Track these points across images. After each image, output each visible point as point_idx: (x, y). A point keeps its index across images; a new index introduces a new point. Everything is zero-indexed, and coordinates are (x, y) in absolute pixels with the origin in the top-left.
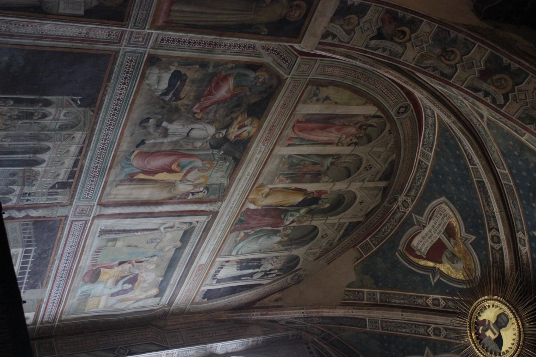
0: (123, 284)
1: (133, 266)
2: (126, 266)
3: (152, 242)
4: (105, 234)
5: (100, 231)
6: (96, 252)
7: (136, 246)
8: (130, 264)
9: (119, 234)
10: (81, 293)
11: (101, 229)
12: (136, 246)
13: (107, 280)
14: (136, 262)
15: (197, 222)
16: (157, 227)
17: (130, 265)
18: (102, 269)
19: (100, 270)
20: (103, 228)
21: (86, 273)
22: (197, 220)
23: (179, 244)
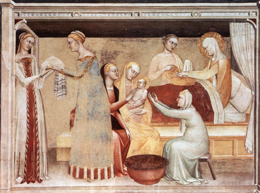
0: (178, 108)
1: (126, 102)
3: (64, 87)
4: (37, 172)
5: (28, 183)
6: (81, 177)
7: (73, 112)
8: (120, 110)
9: (37, 149)
10: (193, 176)
11: (22, 182)
12: (73, 112)
13: (162, 139)
14: (117, 99)
15: (16, 21)
16: (25, 89)
17: (123, 110)
18: (130, 154)
19: (131, 158)
20: (20, 179)
21: (137, 180)
22: (11, 21)
23: (75, 35)
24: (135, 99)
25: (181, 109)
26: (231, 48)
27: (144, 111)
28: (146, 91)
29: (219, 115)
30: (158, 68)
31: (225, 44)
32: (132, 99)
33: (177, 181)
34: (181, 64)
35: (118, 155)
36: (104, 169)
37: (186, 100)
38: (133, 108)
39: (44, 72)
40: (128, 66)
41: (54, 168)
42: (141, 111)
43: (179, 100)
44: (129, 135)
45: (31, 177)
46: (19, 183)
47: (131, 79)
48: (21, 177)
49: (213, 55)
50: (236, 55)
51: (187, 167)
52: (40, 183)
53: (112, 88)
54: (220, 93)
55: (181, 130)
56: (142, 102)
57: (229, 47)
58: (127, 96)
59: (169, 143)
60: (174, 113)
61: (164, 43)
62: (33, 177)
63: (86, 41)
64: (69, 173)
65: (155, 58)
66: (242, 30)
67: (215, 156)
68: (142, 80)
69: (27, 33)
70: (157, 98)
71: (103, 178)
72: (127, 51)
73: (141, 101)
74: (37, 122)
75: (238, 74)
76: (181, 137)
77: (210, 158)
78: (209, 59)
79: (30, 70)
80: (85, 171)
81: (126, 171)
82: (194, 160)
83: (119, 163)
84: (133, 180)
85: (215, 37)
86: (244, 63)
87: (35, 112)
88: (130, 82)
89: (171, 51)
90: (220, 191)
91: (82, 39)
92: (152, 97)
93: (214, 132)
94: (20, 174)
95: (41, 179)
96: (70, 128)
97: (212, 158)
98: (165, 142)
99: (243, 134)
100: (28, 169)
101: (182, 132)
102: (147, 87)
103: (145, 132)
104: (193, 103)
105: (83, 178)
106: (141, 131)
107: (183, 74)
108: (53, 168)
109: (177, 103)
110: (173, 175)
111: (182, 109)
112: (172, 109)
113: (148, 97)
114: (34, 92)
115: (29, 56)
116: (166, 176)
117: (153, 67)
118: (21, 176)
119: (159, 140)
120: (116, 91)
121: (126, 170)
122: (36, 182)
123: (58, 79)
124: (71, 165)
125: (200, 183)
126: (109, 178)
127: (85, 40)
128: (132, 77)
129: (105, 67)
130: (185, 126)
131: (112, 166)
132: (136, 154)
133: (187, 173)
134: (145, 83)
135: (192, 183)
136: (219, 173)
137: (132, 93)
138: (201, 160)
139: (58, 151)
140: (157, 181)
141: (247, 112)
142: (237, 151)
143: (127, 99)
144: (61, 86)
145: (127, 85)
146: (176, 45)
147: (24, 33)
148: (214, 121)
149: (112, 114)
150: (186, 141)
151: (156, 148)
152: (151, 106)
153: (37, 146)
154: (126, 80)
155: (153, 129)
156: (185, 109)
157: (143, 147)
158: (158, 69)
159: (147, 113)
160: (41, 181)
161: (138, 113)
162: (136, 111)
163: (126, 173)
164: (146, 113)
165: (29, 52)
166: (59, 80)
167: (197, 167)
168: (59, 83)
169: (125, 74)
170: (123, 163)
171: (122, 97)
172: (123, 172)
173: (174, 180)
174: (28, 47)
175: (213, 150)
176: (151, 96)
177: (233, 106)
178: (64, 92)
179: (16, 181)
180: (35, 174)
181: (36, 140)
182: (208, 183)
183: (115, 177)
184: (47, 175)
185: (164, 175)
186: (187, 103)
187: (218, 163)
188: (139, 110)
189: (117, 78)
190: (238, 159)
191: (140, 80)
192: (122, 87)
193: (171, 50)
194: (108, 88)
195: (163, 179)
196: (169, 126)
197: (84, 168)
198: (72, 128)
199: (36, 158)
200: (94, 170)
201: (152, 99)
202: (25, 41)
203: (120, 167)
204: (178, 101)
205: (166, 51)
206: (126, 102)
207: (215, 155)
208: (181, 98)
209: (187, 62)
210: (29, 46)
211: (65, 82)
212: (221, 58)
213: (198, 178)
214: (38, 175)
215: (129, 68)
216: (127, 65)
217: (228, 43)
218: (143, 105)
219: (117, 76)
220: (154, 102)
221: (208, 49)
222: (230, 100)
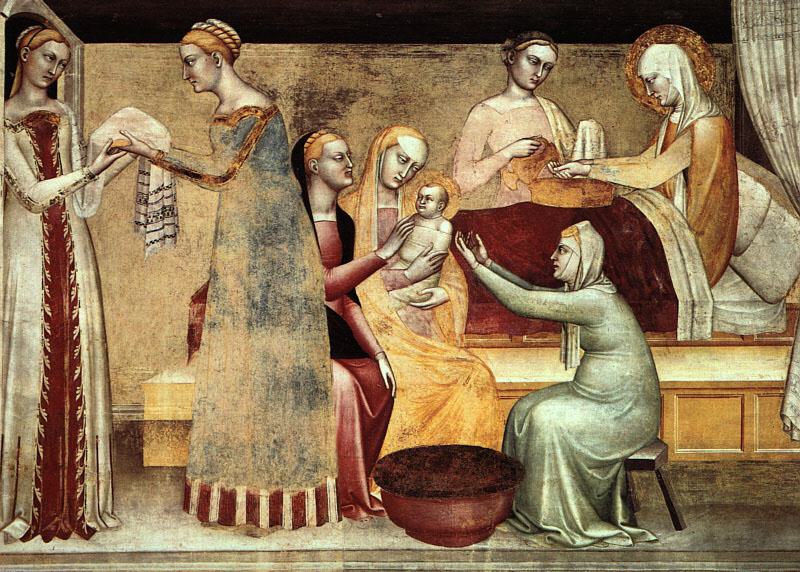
0: (557, 285)
1: (379, 264)
2: (376, 305)
3: (169, 211)
6: (227, 519)
7: (200, 297)
8: (359, 290)
9: (77, 425)
10: (608, 518)
11: (26, 538)
14: (346, 254)
16: (36, 219)
17: (370, 290)
18: (391, 445)
19: (396, 456)
20: (19, 527)
21: (415, 532)
24: (409, 253)
25: (566, 287)
26: (737, 81)
27: (440, 294)
28: (447, 227)
29: (696, 309)
30: (487, 147)
31: (717, 67)
32: (397, 252)
33: (552, 535)
34: (567, 135)
35: (353, 448)
36: (303, 494)
37: (584, 257)
38: (403, 286)
39: (100, 160)
40: (387, 140)
41: (134, 491)
42: (432, 294)
43: (560, 257)
44: (388, 377)
45: (56, 519)
46: (15, 540)
47: (395, 185)
48: (22, 519)
49: (673, 105)
50: (754, 106)
51: (584, 486)
52: (87, 539)
53: (332, 217)
54: (699, 234)
55: (565, 362)
56: (434, 264)
57: (731, 76)
58: (381, 245)
59: (526, 405)
60: (542, 301)
61: (507, 64)
62: (64, 519)
63: (242, 56)
64: (186, 506)
65: (478, 115)
66: (775, 18)
67: (680, 453)
68: (433, 191)
69: (45, 28)
70: (483, 251)
71: (299, 522)
72: (383, 89)
73: (430, 260)
74: (76, 332)
75: (761, 170)
76: (566, 383)
77: (664, 457)
78: (662, 117)
79: (54, 154)
80: (241, 499)
81: (378, 500)
82: (612, 463)
83: (355, 473)
84: (402, 532)
85: (682, 45)
86: (781, 130)
87: (70, 299)
88: (390, 196)
89: (531, 90)
90: (697, 566)
91: (231, 49)
92: (467, 246)
93: (676, 370)
94: (20, 508)
95: (92, 525)
96: (190, 353)
97: (671, 458)
98: (511, 403)
99: (777, 375)
100: (44, 492)
101: (569, 366)
102: (452, 211)
103: (443, 367)
104: (605, 269)
105: (234, 525)
106: (432, 362)
107: (574, 167)
108: (130, 490)
109: (553, 268)
110: (536, 512)
111: (571, 290)
112: (537, 288)
113: (452, 245)
114: (66, 230)
115: (50, 107)
116: (514, 517)
117: (469, 146)
118: (22, 515)
119: (489, 396)
120: (345, 226)
121: (379, 497)
122: (74, 535)
123: (148, 185)
124: (193, 480)
125: (630, 542)
126: (319, 524)
127: (238, 53)
128: (399, 178)
129: (306, 145)
130: (581, 347)
131: (331, 483)
132: (412, 442)
133: (587, 508)
134: (445, 200)
135: (601, 540)
136: (697, 509)
137: (399, 233)
138: (630, 465)
139: (150, 434)
140: (483, 533)
141: (789, 300)
142: (754, 432)
143: (384, 254)
144: (157, 208)
145: (382, 206)
146: (550, 69)
147: (31, 28)
148: (679, 331)
149: (332, 305)
150: (583, 397)
151: (480, 423)
152: (463, 278)
153: (76, 416)
154: (381, 188)
155: (469, 358)
156: (581, 288)
157: (436, 421)
158: (488, 152)
159: (449, 300)
160: (92, 531)
161: (421, 301)
162: (413, 295)
163: (377, 508)
164: (446, 302)
165: (51, 92)
166: (153, 188)
167: (619, 489)
168: (152, 199)
169: (374, 172)
170: (368, 475)
171: (366, 247)
172: (368, 504)
173: (542, 531)
174: (48, 75)
175: (675, 429)
176: (465, 243)
177: (744, 278)
178: (169, 230)
179: (6, 534)
180: (71, 507)
181: (73, 395)
182: (656, 541)
183: (340, 520)
184: (112, 513)
185: (508, 515)
186: (586, 266)
187: (692, 474)
188: (424, 292)
189: (348, 181)
190: (758, 463)
191: (426, 191)
192: (368, 209)
193: (532, 86)
194: (317, 217)
195: (503, 528)
196: (525, 346)
197: (237, 488)
198: (196, 353)
199: (73, 456)
200: (271, 497)
201: (469, 255)
202: (38, 53)
203: (359, 488)
204: (557, 260)
205: (515, 89)
206: (379, 264)
207: (681, 446)
208: (566, 251)
209: (588, 129)
210: (51, 74)
211: (173, 197)
212: (701, 114)
213: (622, 524)
214: (80, 513)
215: (388, 148)
216: (381, 138)
217: (724, 64)
218: (437, 275)
219: (349, 175)
220: (475, 265)
221: (659, 82)
222: (733, 258)
